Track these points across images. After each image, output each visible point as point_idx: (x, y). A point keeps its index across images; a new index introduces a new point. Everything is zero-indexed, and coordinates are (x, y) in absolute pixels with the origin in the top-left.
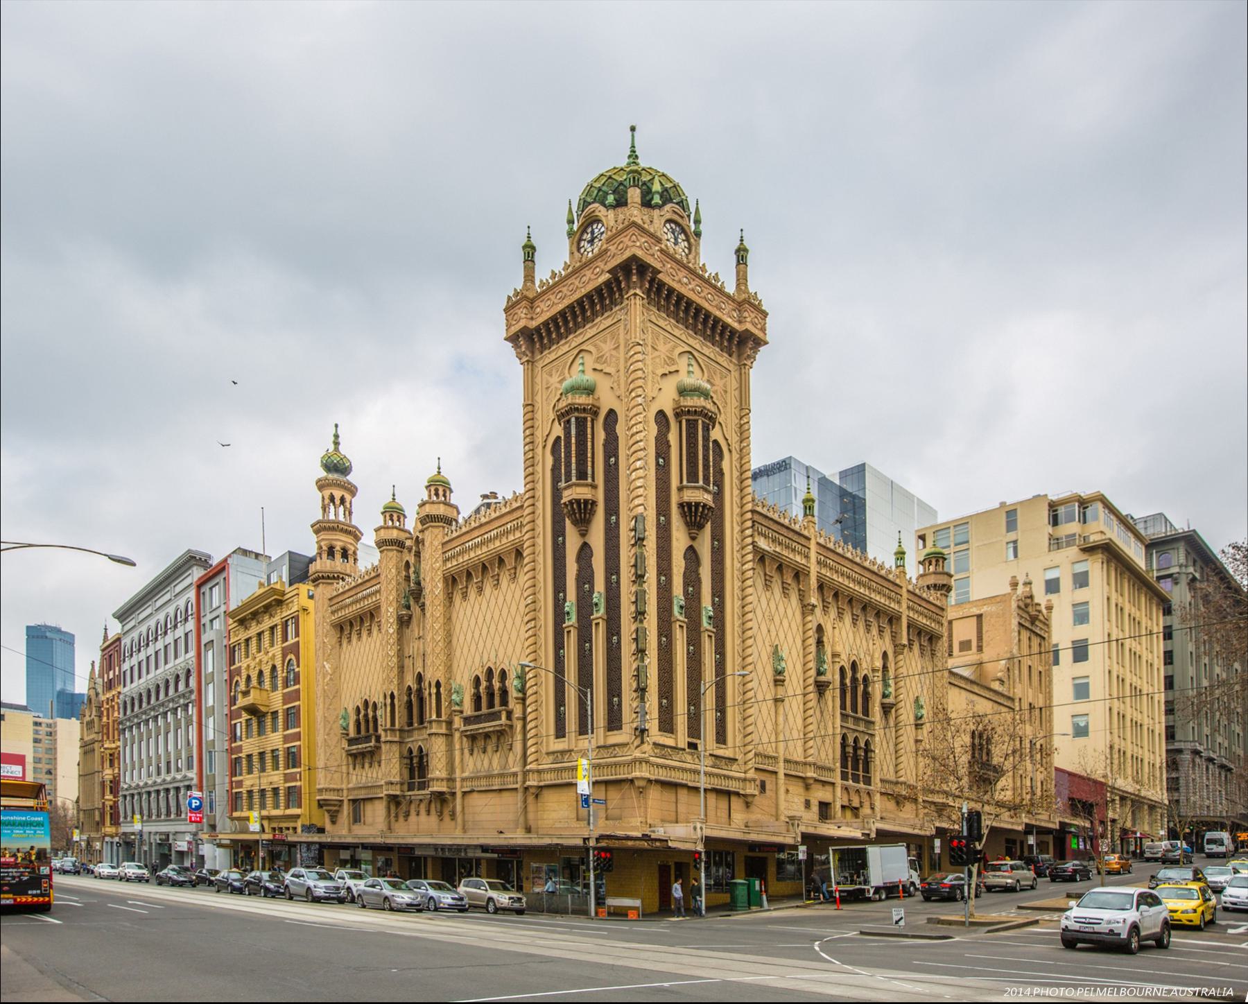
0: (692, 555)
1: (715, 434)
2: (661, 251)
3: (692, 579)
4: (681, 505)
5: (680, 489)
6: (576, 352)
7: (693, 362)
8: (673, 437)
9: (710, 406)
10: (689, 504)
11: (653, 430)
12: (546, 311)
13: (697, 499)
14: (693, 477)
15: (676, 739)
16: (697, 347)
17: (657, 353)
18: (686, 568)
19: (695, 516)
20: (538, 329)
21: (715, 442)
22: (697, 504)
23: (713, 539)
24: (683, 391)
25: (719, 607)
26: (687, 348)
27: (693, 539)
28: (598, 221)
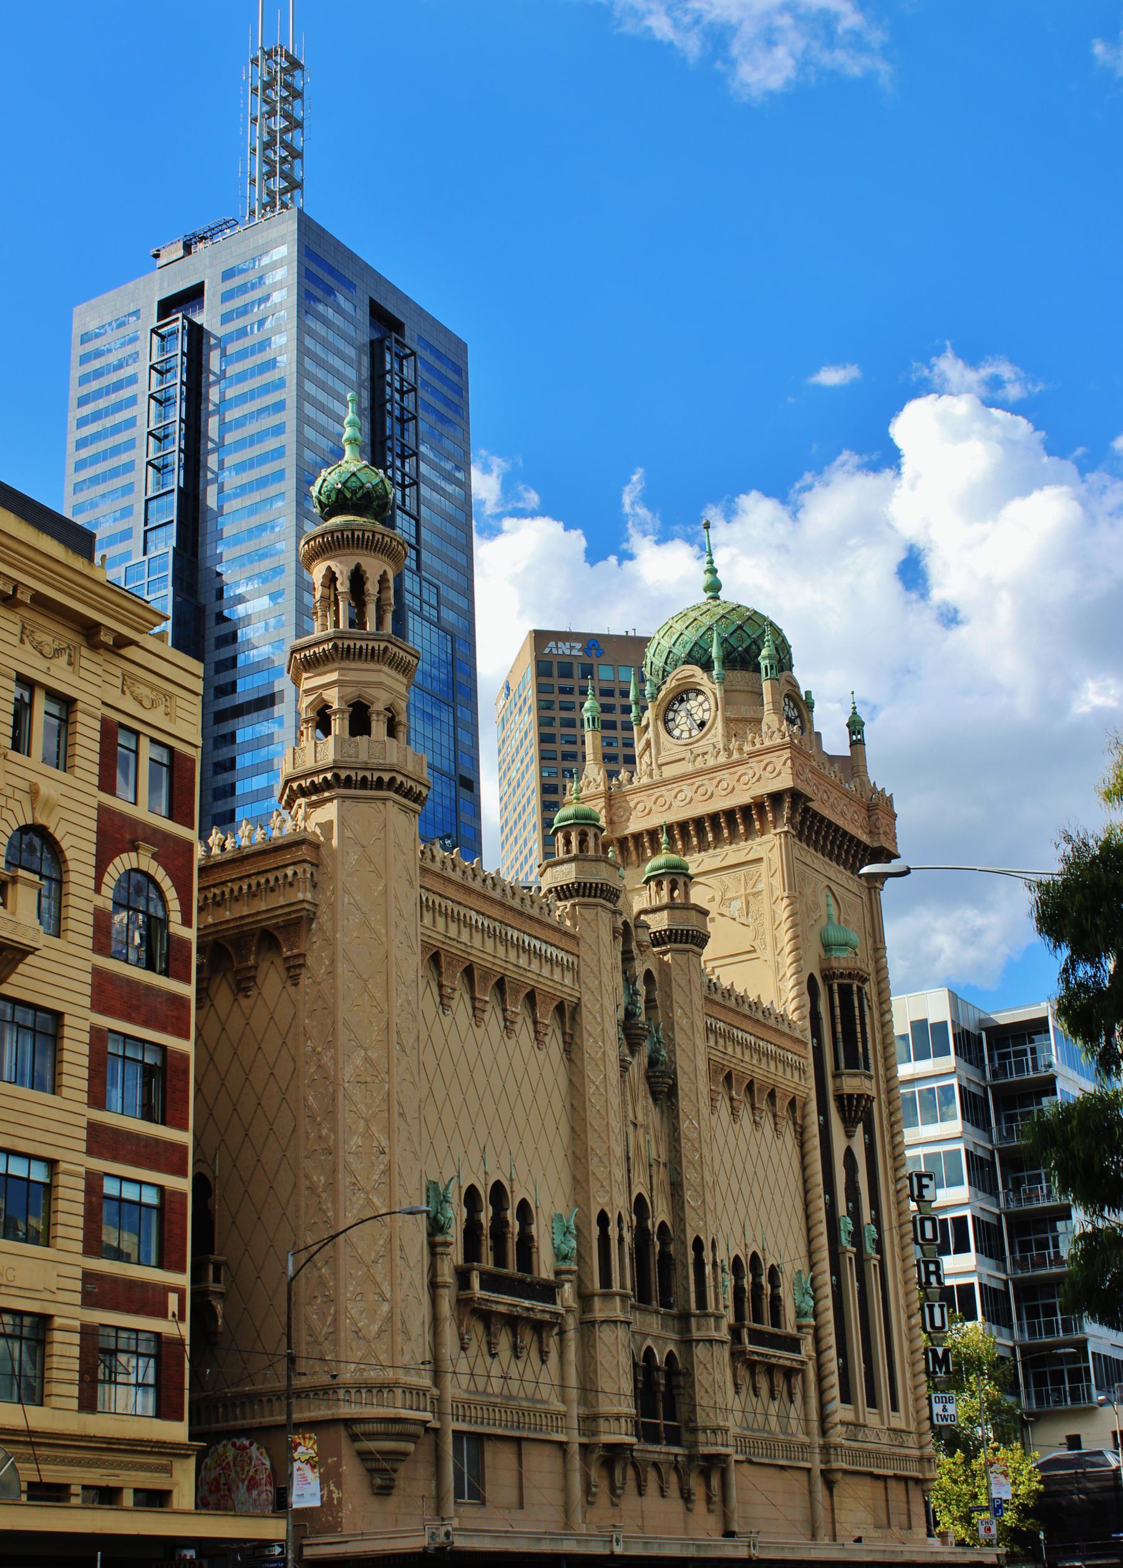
4: (839, 1098)
5: (837, 1075)
7: (831, 901)
10: (850, 1096)
22: (860, 1096)
28: (699, 692)
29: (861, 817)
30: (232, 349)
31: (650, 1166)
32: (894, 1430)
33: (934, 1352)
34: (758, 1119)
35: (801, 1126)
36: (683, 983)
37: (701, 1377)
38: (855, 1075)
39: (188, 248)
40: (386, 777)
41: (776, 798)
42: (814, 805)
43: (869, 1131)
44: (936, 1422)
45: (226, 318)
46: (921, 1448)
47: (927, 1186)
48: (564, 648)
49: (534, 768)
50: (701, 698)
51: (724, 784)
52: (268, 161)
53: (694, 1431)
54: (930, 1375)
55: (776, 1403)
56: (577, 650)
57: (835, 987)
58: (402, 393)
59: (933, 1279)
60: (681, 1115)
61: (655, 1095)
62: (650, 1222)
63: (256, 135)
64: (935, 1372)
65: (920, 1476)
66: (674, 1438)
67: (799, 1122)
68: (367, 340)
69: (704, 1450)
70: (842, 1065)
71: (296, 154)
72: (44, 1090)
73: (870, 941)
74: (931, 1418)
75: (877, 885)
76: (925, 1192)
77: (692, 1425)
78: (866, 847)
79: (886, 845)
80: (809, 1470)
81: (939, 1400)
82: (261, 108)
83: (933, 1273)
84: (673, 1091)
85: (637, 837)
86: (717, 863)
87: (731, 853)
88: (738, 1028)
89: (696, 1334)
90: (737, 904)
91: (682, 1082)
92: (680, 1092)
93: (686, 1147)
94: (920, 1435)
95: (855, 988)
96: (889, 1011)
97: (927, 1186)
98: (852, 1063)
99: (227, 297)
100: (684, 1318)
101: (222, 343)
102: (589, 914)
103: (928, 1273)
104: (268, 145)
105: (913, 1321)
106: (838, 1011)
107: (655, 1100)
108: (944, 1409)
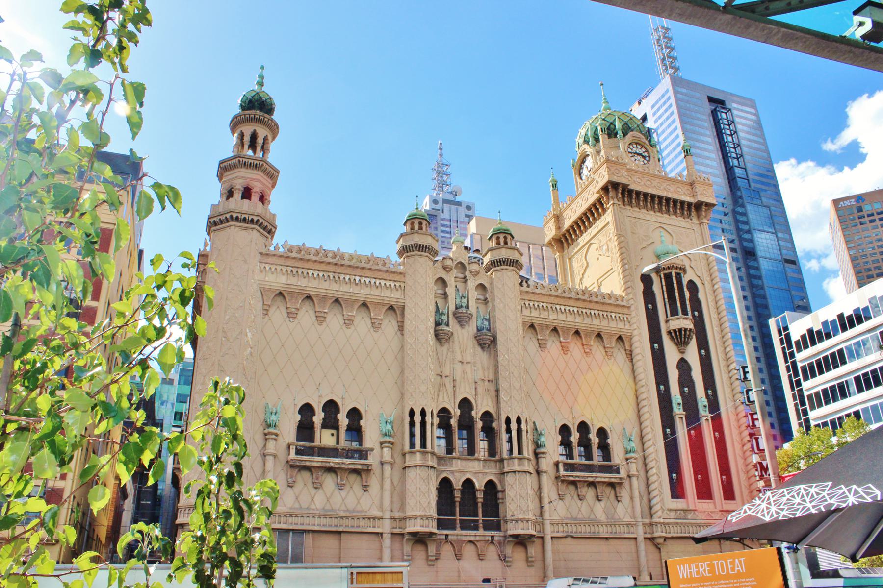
0: (683, 366)
4: (669, 333)
5: (667, 322)
7: (663, 233)
8: (657, 288)
10: (675, 331)
11: (641, 287)
14: (674, 312)
15: (687, 503)
18: (680, 375)
19: (680, 338)
20: (564, 235)
22: (680, 330)
27: (683, 353)
30: (659, 132)
36: (500, 286)
37: (510, 493)
39: (639, 103)
40: (228, 216)
41: (605, 189)
42: (632, 187)
45: (656, 122)
48: (847, 203)
49: (846, 252)
52: (665, 65)
53: (506, 522)
55: (603, 503)
56: (853, 202)
58: (729, 125)
60: (499, 353)
61: (482, 346)
62: (473, 413)
63: (658, 57)
66: (498, 527)
67: (627, 348)
68: (710, 111)
69: (510, 532)
71: (675, 59)
72: (719, 414)
78: (689, 204)
80: (636, 538)
82: (658, 48)
84: (494, 341)
85: (568, 231)
86: (596, 231)
87: (600, 224)
89: (506, 469)
90: (605, 248)
95: (673, 274)
98: (674, 312)
99: (654, 114)
100: (502, 460)
101: (656, 131)
102: (410, 260)
104: (663, 60)
105: (745, 448)
107: (482, 348)
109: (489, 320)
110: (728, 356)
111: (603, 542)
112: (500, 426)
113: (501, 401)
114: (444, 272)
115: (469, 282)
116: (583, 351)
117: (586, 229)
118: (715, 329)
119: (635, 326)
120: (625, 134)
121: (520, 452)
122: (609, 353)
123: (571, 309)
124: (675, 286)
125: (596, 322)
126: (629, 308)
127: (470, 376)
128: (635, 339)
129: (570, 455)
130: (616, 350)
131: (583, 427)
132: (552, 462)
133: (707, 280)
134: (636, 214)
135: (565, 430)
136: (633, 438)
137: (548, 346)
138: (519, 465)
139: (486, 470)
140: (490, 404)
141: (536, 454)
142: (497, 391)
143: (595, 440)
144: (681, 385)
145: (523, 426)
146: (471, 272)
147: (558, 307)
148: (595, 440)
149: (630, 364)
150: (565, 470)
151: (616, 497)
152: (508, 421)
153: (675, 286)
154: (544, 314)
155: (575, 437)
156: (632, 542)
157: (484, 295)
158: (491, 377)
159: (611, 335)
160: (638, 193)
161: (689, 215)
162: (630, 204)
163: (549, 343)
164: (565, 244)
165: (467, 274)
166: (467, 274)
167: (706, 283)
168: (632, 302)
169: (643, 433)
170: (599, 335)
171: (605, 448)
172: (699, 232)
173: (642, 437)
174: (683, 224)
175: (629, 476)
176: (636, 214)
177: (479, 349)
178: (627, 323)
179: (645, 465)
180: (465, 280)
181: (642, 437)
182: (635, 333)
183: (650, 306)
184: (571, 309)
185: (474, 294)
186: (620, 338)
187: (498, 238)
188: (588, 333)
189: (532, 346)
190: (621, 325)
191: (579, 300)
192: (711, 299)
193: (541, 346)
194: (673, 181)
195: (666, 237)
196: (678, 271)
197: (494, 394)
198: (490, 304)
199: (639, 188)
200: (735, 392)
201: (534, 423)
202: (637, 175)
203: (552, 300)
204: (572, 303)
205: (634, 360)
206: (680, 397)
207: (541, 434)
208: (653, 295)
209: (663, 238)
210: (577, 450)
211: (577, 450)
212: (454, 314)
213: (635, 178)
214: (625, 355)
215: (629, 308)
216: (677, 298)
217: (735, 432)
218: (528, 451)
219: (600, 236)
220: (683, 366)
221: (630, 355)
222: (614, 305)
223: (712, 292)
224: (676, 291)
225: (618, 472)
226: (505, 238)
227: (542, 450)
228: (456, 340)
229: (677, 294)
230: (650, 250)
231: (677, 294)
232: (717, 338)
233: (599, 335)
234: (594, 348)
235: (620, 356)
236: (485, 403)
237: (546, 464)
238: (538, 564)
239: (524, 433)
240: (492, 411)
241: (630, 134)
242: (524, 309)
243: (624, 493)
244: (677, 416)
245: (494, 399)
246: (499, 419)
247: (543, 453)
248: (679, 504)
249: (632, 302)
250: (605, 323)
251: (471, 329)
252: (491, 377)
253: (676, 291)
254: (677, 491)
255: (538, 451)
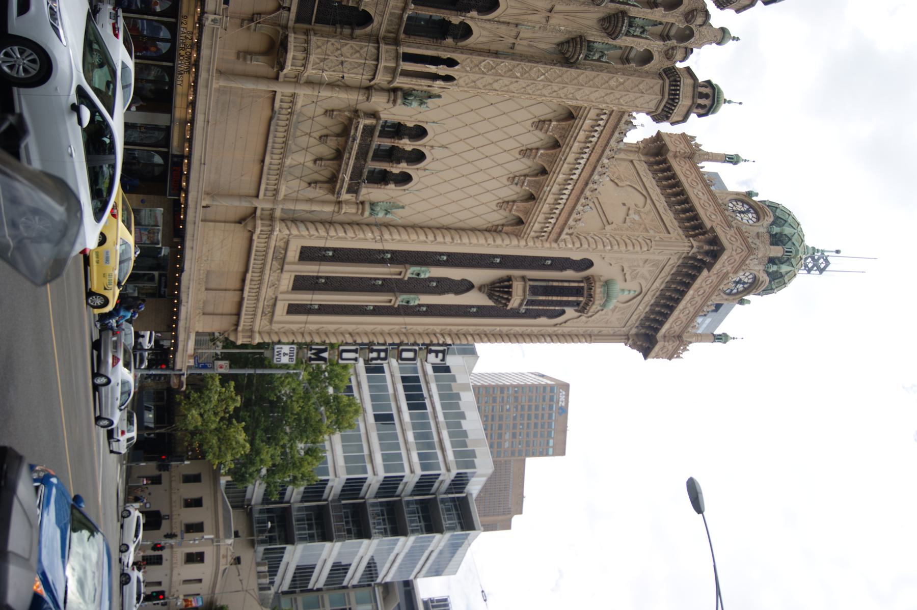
0: (465, 286)
1: (570, 312)
2: (727, 274)
3: (445, 286)
4: (509, 279)
5: (523, 278)
6: (645, 193)
7: (632, 294)
8: (569, 274)
9: (594, 308)
10: (510, 287)
11: (576, 256)
12: (680, 168)
13: (514, 293)
14: (534, 290)
16: (646, 299)
17: (641, 264)
18: (453, 280)
20: (665, 161)
21: (563, 312)
22: (510, 293)
23: (478, 307)
24: (607, 284)
25: (415, 311)
26: (644, 290)
28: (758, 219)
29: (677, 329)
31: (517, 25)
32: (274, 305)
33: (325, 350)
34: (517, 179)
35: (501, 231)
36: (641, 87)
37: (348, 47)
38: (524, 291)
42: (705, 272)
43: (482, 312)
44: (277, 346)
46: (259, 333)
47: (437, 357)
48: (562, 398)
50: (755, 220)
51: (714, 217)
53: (306, 33)
54: (309, 346)
55: (310, 164)
57: (582, 285)
59: (374, 355)
60: (548, 67)
62: (474, 14)
64: (311, 349)
65: (240, 328)
67: (505, 228)
69: (292, 38)
70: (531, 283)
73: (596, 331)
74: (279, 342)
75: (630, 342)
76: (433, 355)
77: (312, 33)
78: (657, 330)
79: (657, 348)
80: (257, 196)
81: (291, 351)
83: (379, 355)
85: (669, 169)
86: (661, 211)
88: (588, 159)
89: (383, 47)
91: (573, 72)
92: (564, 69)
93: (526, 65)
94: (269, 333)
95: (581, 299)
96: (552, 341)
97: (437, 357)
98: (534, 290)
100: (396, 42)
103: (379, 351)
105: (347, 336)
106: (566, 284)
107: (560, 44)
108: (285, 354)
109: (599, 60)
110: (462, 337)
111: (258, 157)
112: (447, 48)
113: (481, 58)
114: (690, 8)
115: (661, 43)
116: (517, 174)
117: (667, 196)
118: (498, 328)
119: (531, 244)
120: (769, 274)
121: (405, 74)
122: (505, 205)
123: (577, 172)
124: (565, 298)
125: (551, 199)
126: (556, 241)
127: (530, 17)
128: (515, 242)
129: (383, 134)
130: (506, 213)
131: (418, 157)
132: (380, 109)
133: (559, 330)
134: (667, 269)
135: (420, 132)
136: (389, 216)
137: (537, 132)
138: (385, 67)
139: (386, 16)
140: (481, 39)
141: (395, 90)
142: (496, 54)
143: (396, 169)
144: (439, 280)
145: (439, 83)
146: (673, 48)
147: (585, 156)
148: (396, 169)
149: (485, 227)
150: (365, 126)
151: (316, 182)
152: (451, 63)
153: (565, 298)
154: (582, 136)
155: (407, 144)
156: (253, 192)
157: (634, 60)
158: (518, 49)
159: (527, 212)
160: (694, 278)
161: (642, 325)
162: (683, 265)
163: (540, 134)
164: (652, 159)
165: (674, 42)
166: (674, 42)
167: (556, 329)
168: (562, 244)
169: (392, 229)
170: (531, 198)
171: (382, 178)
172: (618, 333)
173: (387, 225)
174: (634, 317)
175: (339, 203)
176: (667, 269)
177: (562, 38)
178: (538, 234)
179: (350, 224)
180: (665, 37)
181: (387, 225)
182: (523, 243)
183: (549, 262)
184: (577, 172)
185: (639, 45)
186: (520, 222)
187: (706, 96)
188: (540, 186)
189: (542, 111)
190: (537, 227)
191: (586, 184)
192: (535, 330)
193: (540, 124)
194: (692, 320)
195: (626, 296)
196: (582, 305)
197: (493, 47)
198: (620, 66)
199: (699, 281)
200: (417, 336)
201: (439, 96)
202: (715, 281)
203: (598, 150)
204: (585, 174)
205: (487, 234)
206: (427, 275)
207: (422, 103)
208: (563, 269)
209: (626, 293)
210: (387, 143)
211: (387, 143)
212: (624, 13)
213: (714, 278)
214: (496, 223)
215: (556, 241)
216: (550, 298)
217: (369, 328)
218: (401, 82)
219: (653, 213)
220: (465, 286)
221: (494, 230)
222: (565, 224)
223: (543, 332)
224: (559, 298)
225: (348, 192)
226: (705, 106)
227: (399, 101)
228: (586, 8)
229: (555, 298)
230: (619, 278)
231: (555, 298)
232: (486, 328)
233: (531, 198)
234: (517, 189)
235: (498, 217)
236: (484, 33)
237: (379, 102)
238: (240, 66)
239: (429, 82)
240: (470, 41)
241: (767, 279)
242: (598, 111)
243: (319, 193)
244: (403, 270)
245: (486, 47)
246: (455, 49)
247: (395, 102)
248: (293, 253)
249: (562, 244)
250: (546, 208)
251: (597, 37)
252: (518, 49)
253: (559, 298)
254: (307, 254)
255: (400, 94)
